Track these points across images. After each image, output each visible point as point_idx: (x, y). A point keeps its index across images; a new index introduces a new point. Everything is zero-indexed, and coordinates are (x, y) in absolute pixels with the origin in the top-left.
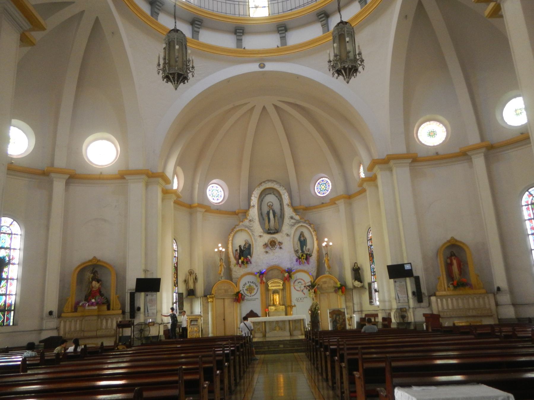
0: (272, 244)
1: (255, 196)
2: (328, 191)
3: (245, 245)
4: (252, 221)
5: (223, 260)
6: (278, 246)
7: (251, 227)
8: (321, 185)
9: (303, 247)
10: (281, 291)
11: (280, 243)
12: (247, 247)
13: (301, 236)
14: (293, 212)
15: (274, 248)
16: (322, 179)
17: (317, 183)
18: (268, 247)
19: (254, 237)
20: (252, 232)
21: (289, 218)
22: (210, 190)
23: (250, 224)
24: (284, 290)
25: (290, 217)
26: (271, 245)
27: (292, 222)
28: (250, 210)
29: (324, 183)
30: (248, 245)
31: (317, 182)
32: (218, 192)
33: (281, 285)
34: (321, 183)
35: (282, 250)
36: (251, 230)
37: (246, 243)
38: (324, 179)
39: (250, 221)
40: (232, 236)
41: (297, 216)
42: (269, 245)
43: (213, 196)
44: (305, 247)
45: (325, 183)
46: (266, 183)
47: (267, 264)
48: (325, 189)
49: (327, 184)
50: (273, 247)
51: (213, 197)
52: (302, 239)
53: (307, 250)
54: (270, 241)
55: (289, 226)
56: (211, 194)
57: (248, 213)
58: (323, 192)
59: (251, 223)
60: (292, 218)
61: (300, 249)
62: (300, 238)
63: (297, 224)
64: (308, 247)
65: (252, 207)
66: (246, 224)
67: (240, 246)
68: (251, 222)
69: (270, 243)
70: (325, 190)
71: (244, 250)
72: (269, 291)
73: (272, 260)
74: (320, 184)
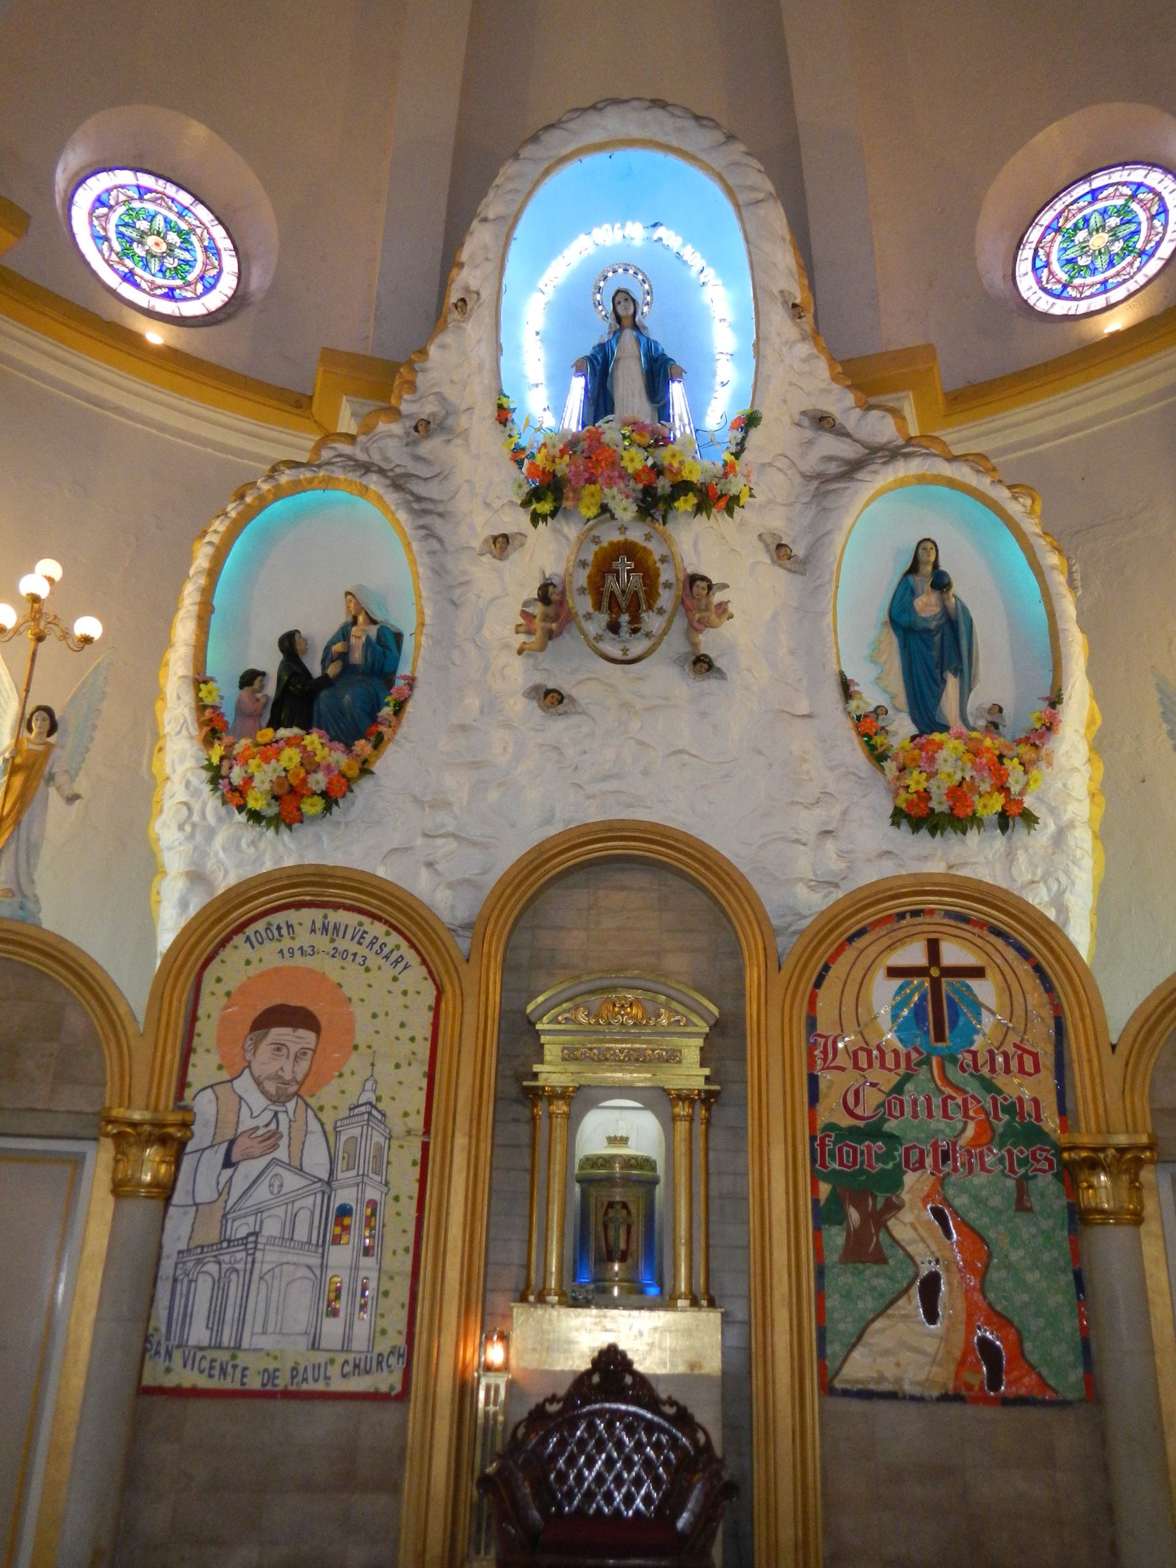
0: (610, 578)
1: (485, 220)
2: (1152, 255)
3: (344, 634)
4: (442, 428)
5: (53, 728)
6: (675, 643)
7: (426, 479)
8: (1076, 228)
9: (944, 681)
10: (691, 1119)
11: (710, 587)
12: (357, 657)
13: (923, 582)
14: (835, 386)
15: (638, 647)
16: (1083, 188)
17: (1034, 235)
18: (569, 641)
19: (432, 553)
20: (426, 512)
21: (797, 418)
22: (99, 202)
23: (418, 458)
24: (725, 1115)
25: (804, 413)
26: (598, 606)
27: (830, 459)
28: (433, 350)
29: (1104, 212)
30: (373, 631)
31: (1031, 223)
32: (187, 250)
33: (691, 1049)
34: (1079, 216)
35: (710, 684)
36: (419, 499)
37: (355, 622)
38: (1099, 181)
39: (423, 428)
40: (215, 539)
41: (875, 413)
42: (582, 604)
43: (126, 253)
44: (952, 684)
45: (1121, 201)
46: (601, 109)
47: (548, 821)
48: (1117, 247)
49: (1134, 206)
50: (625, 618)
51: (128, 262)
52: (926, 605)
53: (982, 723)
54: (590, 558)
55: (798, 480)
56: (112, 234)
57: (414, 371)
58: (1099, 277)
59: (427, 448)
60: (822, 422)
61: (902, 700)
62: (904, 595)
63: (884, 463)
64: (980, 698)
65: (456, 315)
66: (376, 458)
67: (289, 644)
68: (428, 435)
69: (597, 588)
70: (1127, 251)
71: (325, 681)
72: (540, 1111)
73: (607, 778)
74: (1069, 225)
